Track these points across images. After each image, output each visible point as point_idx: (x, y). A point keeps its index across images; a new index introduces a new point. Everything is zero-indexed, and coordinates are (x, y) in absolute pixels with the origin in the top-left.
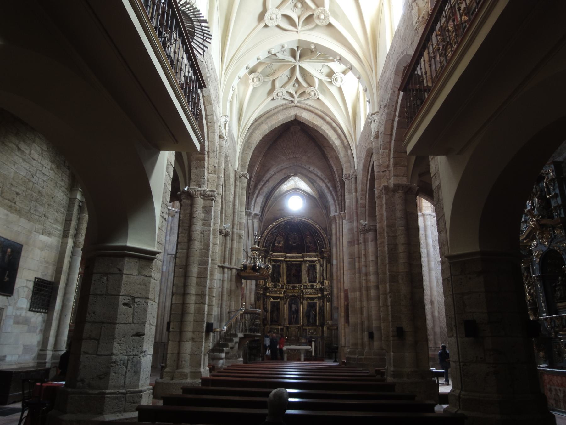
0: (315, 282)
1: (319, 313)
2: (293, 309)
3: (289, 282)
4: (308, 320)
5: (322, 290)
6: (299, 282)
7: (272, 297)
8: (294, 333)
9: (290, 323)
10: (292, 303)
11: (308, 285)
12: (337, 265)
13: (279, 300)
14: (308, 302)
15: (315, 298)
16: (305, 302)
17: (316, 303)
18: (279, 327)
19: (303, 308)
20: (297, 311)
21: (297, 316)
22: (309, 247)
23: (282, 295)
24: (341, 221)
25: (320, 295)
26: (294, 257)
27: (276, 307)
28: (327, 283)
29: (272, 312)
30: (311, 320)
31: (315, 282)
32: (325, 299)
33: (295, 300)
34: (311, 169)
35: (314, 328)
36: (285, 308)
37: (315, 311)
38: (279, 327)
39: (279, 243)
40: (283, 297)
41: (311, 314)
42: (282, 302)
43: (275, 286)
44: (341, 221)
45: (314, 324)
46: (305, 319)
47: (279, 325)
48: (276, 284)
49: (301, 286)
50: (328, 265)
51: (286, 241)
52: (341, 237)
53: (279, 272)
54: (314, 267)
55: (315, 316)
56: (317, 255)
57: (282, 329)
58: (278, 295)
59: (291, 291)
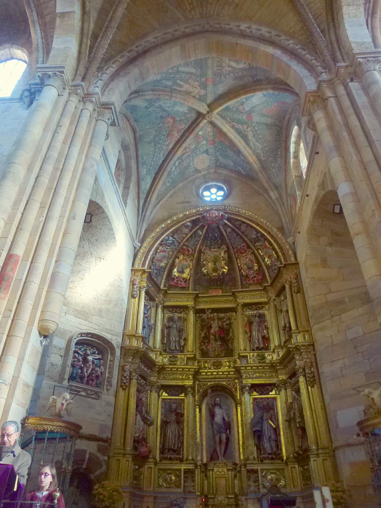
0: (267, 348)
1: (289, 421)
2: (218, 419)
3: (204, 354)
4: (259, 447)
5: (288, 358)
6: (229, 353)
7: (166, 388)
8: (223, 482)
9: (213, 457)
10: (216, 405)
11: (252, 356)
12: (355, 194)
13: (182, 396)
14: (255, 399)
15: (272, 386)
16: (248, 399)
17: (275, 399)
18: (183, 467)
19: (244, 411)
20: (227, 426)
21: (228, 439)
22: (247, 276)
23: (189, 383)
24: (341, 90)
25: (282, 377)
26: (216, 300)
27: (174, 415)
28: (299, 339)
29: (165, 423)
30: (267, 445)
31: (267, 348)
32: (302, 379)
33: (220, 393)
34: (243, 26)
35: (278, 465)
36: (196, 418)
37: (275, 419)
38: (183, 467)
39: (182, 272)
40: (193, 388)
41: (265, 427)
42: (189, 401)
43: (173, 362)
44: (341, 90)
45: (276, 455)
46: (251, 442)
47: (181, 461)
48: (174, 357)
49: (235, 362)
50: (299, 295)
51: (198, 265)
52: (353, 120)
53: (180, 331)
54: (261, 317)
55: (276, 430)
56: (265, 289)
57: (189, 473)
58: (180, 383)
59: (209, 371)
